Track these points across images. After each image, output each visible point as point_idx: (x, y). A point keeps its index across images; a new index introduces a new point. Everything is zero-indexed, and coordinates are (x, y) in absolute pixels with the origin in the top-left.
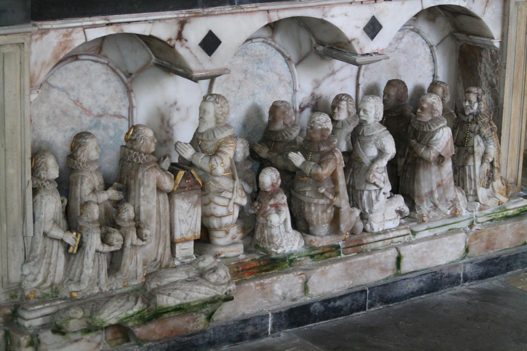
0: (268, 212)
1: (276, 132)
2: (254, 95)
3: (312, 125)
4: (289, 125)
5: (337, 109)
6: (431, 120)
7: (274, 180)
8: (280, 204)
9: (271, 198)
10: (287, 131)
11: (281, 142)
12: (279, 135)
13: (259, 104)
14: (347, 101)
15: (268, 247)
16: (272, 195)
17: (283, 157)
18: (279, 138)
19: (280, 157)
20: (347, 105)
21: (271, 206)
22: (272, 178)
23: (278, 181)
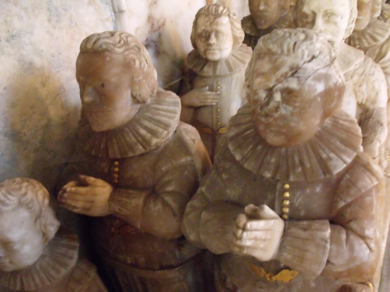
1: (117, 132)
2: (12, 37)
3: (293, 84)
4: (149, 101)
5: (213, 36)
6: (369, 26)
10: (151, 119)
12: (131, 139)
13: (37, 61)
14: (229, 15)
17: (166, 204)
18: (131, 148)
19: (156, 208)
20: (232, 23)
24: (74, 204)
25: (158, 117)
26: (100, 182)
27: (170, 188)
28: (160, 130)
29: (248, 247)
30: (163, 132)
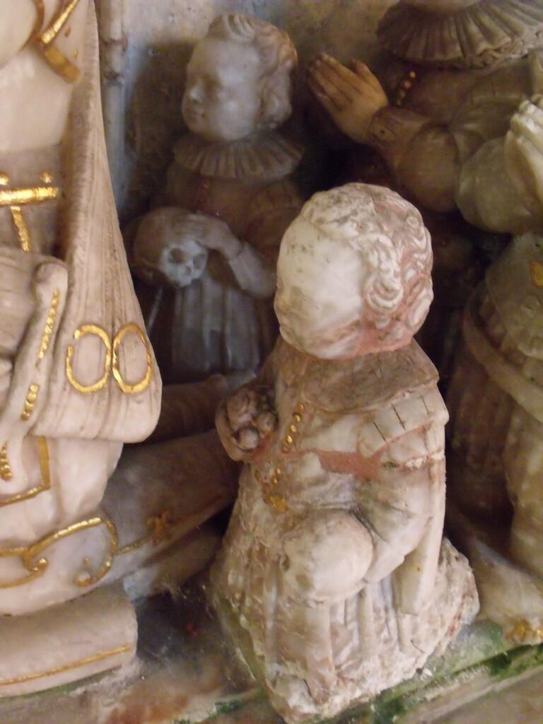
0: (306, 495)
7: (388, 291)
8: (392, 465)
9: (342, 413)
10: (495, 16)
11: (454, 68)
15: (271, 669)
16: (360, 387)
17: (452, 143)
18: (444, 48)
19: (436, 141)
21: (334, 463)
22: (368, 269)
23: (408, 303)
24: (323, 82)
25: (507, 16)
26: (374, 81)
27: (471, 126)
28: (501, 33)
29: (529, 136)
30: (503, 37)
